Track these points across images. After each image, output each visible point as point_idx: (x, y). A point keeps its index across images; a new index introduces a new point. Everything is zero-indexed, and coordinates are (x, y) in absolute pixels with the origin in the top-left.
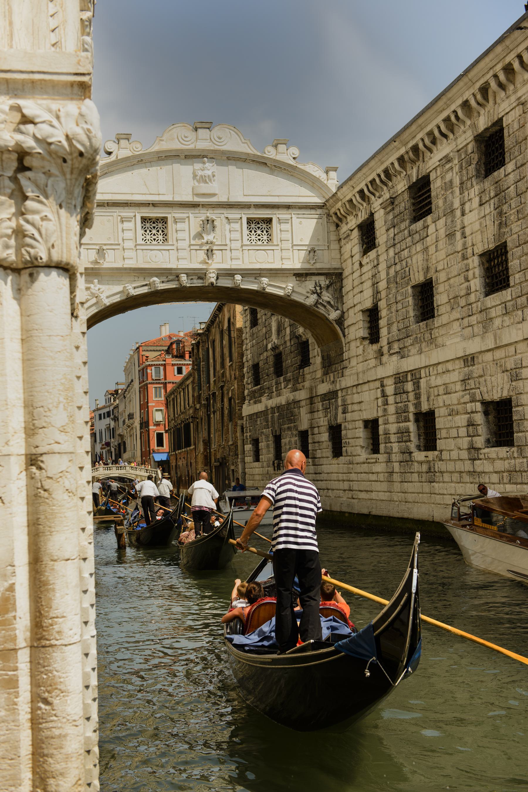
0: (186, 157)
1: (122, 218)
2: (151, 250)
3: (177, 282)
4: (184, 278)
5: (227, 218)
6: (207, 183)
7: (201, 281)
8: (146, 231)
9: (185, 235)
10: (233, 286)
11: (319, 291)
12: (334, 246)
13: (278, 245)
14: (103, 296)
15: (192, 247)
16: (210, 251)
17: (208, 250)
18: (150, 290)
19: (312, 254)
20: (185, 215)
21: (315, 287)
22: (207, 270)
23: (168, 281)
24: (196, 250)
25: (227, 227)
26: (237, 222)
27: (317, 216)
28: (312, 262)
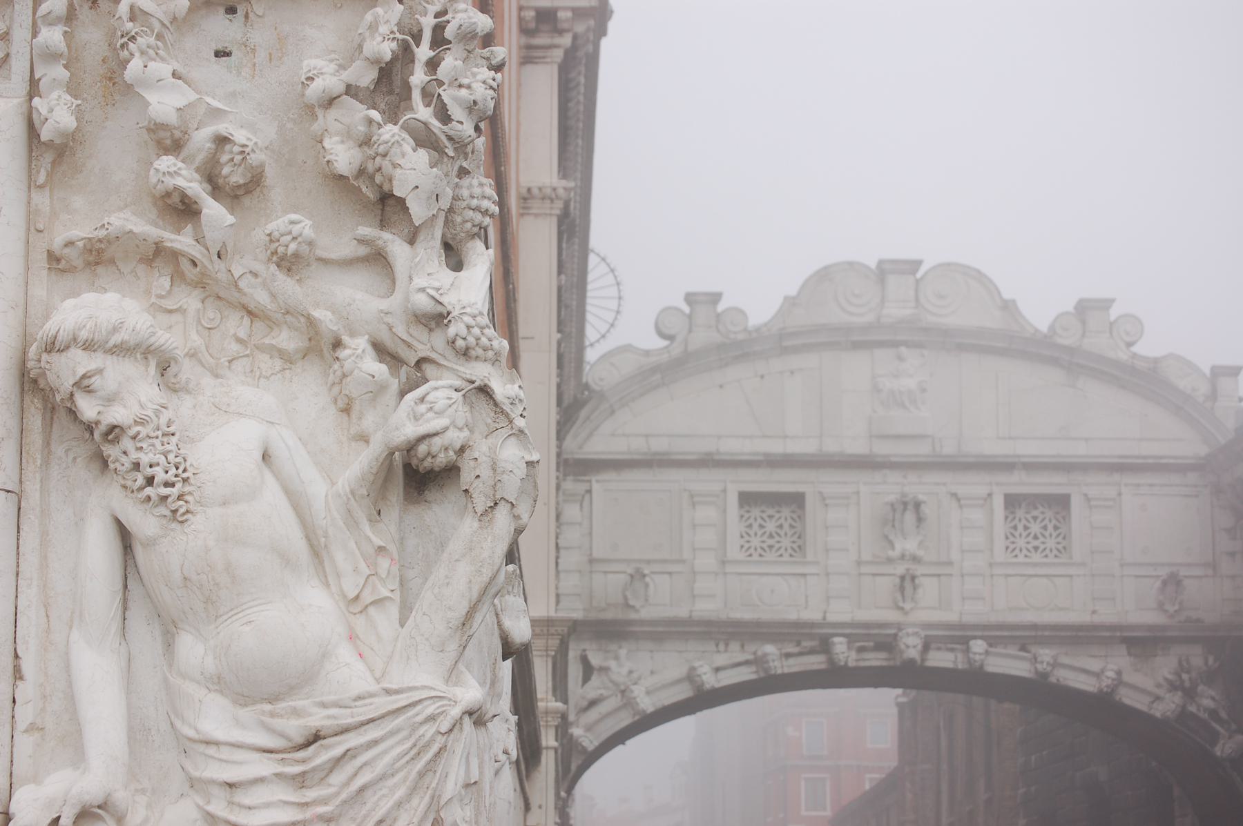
0: (857, 346)
1: (692, 496)
4: (840, 647)
5: (954, 495)
7: (883, 655)
8: (750, 526)
10: (966, 666)
11: (1187, 684)
14: (638, 692)
15: (864, 569)
16: (908, 579)
17: (903, 578)
18: (754, 677)
22: (900, 627)
23: (801, 654)
24: (875, 575)
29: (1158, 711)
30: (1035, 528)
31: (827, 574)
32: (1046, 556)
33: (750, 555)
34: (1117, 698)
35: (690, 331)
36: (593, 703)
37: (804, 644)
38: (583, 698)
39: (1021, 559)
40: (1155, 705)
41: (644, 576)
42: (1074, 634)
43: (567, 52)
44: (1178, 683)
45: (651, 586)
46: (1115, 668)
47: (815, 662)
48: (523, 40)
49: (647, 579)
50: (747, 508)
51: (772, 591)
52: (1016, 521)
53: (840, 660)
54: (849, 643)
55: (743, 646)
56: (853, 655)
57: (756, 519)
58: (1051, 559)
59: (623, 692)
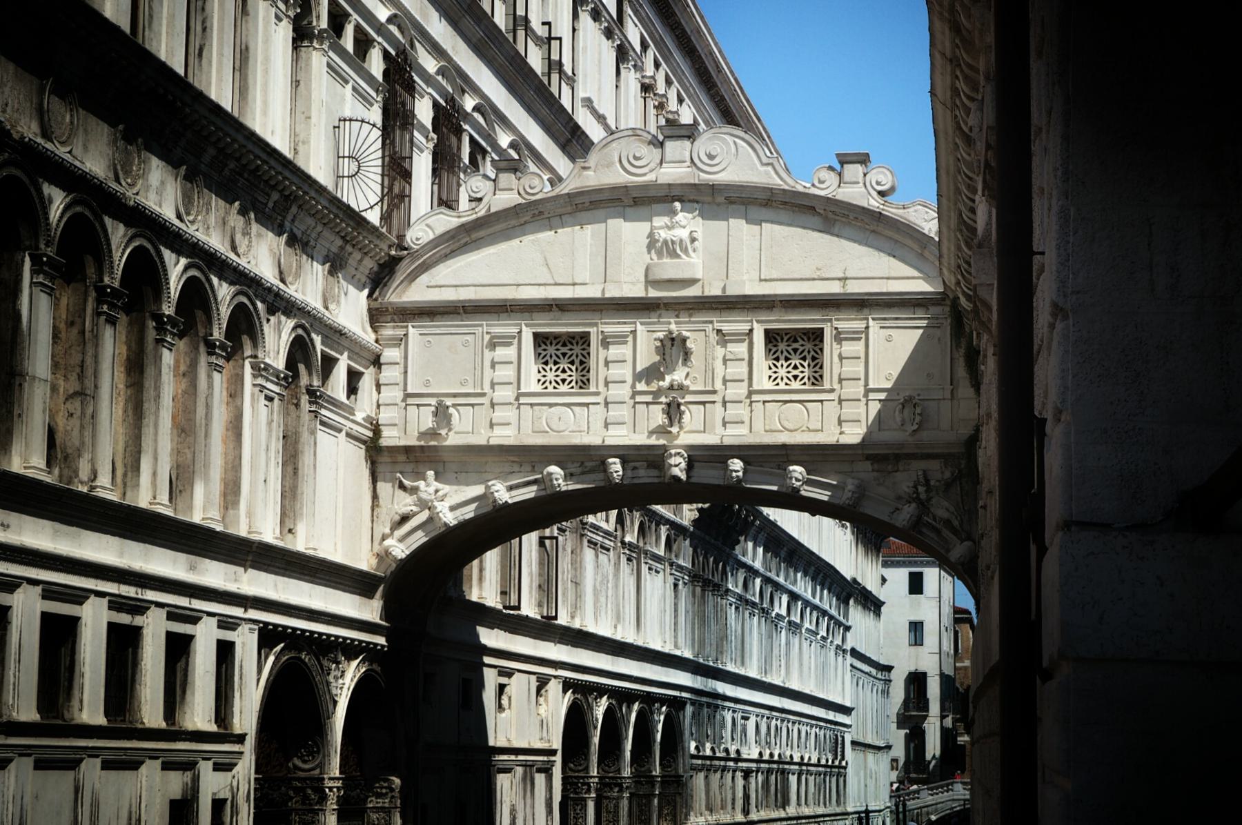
1: (492, 338)
2: (551, 405)
3: (601, 476)
4: (615, 466)
5: (719, 331)
6: (678, 256)
7: (654, 472)
9: (625, 372)
11: (923, 496)
12: (966, 391)
13: (832, 391)
15: (638, 399)
16: (674, 406)
17: (669, 405)
18: (543, 493)
20: (628, 328)
21: (915, 487)
22: (664, 448)
23: (583, 473)
24: (647, 403)
25: (720, 352)
26: (743, 341)
27: (924, 323)
31: (607, 404)
32: (804, 384)
33: (546, 388)
34: (861, 510)
35: (495, 194)
36: (405, 519)
37: (587, 464)
38: (396, 513)
39: (782, 386)
40: (896, 513)
41: (448, 407)
42: (821, 452)
44: (915, 495)
46: (856, 482)
49: (452, 410)
50: (544, 347)
51: (560, 418)
52: (779, 353)
53: (614, 478)
54: (624, 463)
55: (534, 467)
56: (629, 474)
57: (551, 356)
59: (429, 509)
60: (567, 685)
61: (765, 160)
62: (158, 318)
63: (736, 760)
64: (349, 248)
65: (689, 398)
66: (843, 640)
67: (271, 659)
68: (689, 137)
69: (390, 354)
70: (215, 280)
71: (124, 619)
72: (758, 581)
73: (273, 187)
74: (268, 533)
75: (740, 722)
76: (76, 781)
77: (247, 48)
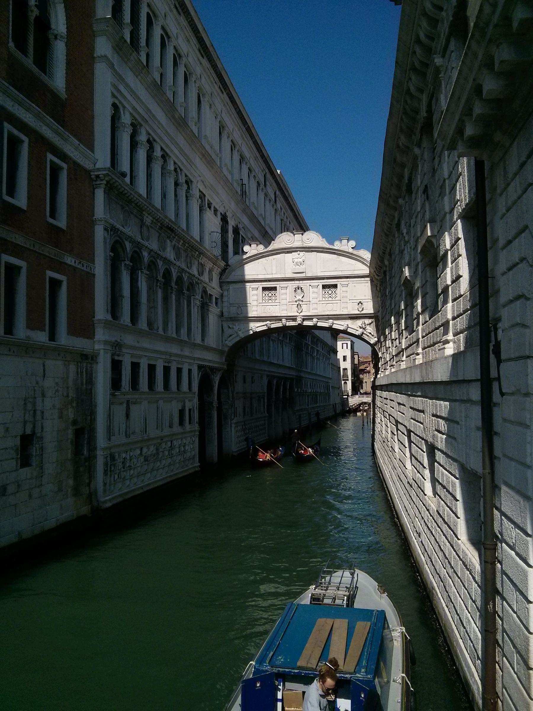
4: (284, 321)
5: (310, 285)
7: (294, 322)
11: (364, 327)
16: (299, 306)
17: (298, 305)
19: (360, 304)
20: (286, 285)
22: (297, 316)
28: (360, 310)
29: (357, 333)
30: (330, 292)
39: (327, 299)
43: (106, 185)
45: (242, 309)
46: (347, 324)
47: (279, 325)
48: (94, 183)
54: (287, 319)
56: (287, 323)
58: (334, 299)
60: (268, 376)
61: (322, 240)
62: (171, 287)
63: (306, 393)
64: (215, 266)
65: (303, 303)
66: (329, 361)
67: (201, 373)
68: (302, 234)
69: (225, 293)
70: (184, 275)
71: (166, 365)
72: (310, 348)
73: (197, 251)
74: (198, 341)
75: (306, 382)
76: (157, 406)
77: (188, 214)
